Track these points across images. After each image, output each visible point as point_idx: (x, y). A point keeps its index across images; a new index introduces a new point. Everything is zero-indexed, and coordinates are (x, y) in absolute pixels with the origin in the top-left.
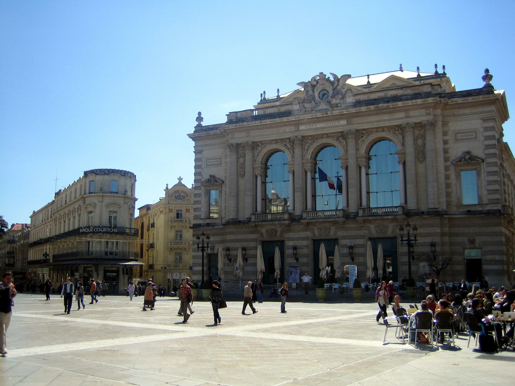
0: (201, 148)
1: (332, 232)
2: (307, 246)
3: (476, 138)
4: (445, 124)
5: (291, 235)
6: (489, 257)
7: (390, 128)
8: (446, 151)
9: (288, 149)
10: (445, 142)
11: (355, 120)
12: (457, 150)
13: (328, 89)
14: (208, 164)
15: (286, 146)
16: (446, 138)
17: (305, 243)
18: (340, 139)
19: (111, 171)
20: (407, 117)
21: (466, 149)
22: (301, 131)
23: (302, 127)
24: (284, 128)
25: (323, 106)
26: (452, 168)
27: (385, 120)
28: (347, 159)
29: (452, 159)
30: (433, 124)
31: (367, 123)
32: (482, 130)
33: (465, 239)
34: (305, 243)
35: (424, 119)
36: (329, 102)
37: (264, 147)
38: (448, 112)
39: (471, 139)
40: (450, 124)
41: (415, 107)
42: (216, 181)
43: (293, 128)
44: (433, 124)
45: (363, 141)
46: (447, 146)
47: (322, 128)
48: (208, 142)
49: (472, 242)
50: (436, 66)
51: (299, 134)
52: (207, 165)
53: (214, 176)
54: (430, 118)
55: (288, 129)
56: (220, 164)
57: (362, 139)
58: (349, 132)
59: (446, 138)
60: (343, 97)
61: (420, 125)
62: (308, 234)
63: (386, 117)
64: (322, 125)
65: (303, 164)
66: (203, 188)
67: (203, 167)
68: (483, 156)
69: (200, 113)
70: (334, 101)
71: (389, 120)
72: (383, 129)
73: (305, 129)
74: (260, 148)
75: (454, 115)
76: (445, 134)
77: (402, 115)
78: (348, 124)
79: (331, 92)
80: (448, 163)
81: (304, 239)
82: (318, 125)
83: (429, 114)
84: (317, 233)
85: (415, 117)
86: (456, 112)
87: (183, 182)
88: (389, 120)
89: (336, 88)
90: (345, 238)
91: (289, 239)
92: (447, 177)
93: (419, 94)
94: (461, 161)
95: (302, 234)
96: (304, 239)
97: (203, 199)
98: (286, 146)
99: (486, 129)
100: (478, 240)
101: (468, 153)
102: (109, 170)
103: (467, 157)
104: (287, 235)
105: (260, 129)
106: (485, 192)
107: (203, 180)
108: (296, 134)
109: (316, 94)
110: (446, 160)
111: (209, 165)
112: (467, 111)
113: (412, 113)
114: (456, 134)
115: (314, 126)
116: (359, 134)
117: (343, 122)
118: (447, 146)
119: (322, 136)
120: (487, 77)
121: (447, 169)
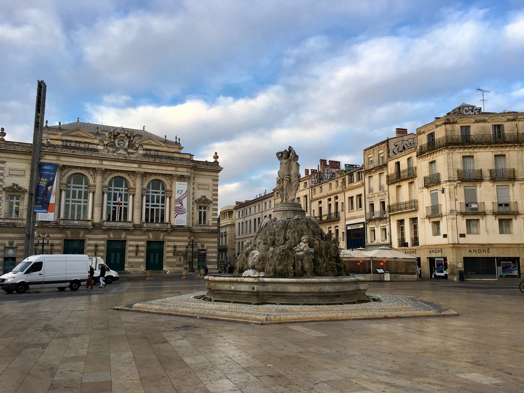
1: (123, 236)
2: (103, 245)
3: (208, 189)
4: (194, 178)
5: (91, 236)
6: (210, 255)
7: (163, 175)
9: (91, 175)
11: (144, 166)
14: (11, 173)
16: (194, 186)
25: (121, 151)
26: (195, 204)
28: (135, 189)
29: (196, 198)
32: (212, 185)
34: (103, 242)
36: (126, 150)
37: (70, 171)
38: (196, 172)
39: (206, 189)
41: (182, 166)
42: (20, 189)
43: (98, 162)
44: (189, 178)
48: (13, 156)
49: (203, 246)
50: (176, 137)
51: (103, 167)
52: (10, 174)
53: (17, 185)
54: (189, 174)
55: (94, 162)
56: (24, 175)
57: (145, 178)
59: (194, 186)
60: (137, 149)
62: (105, 236)
63: (164, 168)
66: (4, 193)
67: (5, 175)
70: (130, 150)
72: (160, 174)
77: (173, 169)
79: (127, 143)
82: (118, 164)
89: (132, 141)
90: (131, 240)
91: (90, 239)
92: (193, 209)
93: (184, 158)
95: (100, 236)
100: (206, 245)
104: (88, 236)
105: (70, 157)
106: (211, 219)
107: (4, 187)
108: (100, 166)
109: (116, 142)
111: (13, 175)
113: (179, 169)
115: (114, 164)
116: (145, 175)
117: (136, 165)
119: (118, 171)
120: (216, 157)
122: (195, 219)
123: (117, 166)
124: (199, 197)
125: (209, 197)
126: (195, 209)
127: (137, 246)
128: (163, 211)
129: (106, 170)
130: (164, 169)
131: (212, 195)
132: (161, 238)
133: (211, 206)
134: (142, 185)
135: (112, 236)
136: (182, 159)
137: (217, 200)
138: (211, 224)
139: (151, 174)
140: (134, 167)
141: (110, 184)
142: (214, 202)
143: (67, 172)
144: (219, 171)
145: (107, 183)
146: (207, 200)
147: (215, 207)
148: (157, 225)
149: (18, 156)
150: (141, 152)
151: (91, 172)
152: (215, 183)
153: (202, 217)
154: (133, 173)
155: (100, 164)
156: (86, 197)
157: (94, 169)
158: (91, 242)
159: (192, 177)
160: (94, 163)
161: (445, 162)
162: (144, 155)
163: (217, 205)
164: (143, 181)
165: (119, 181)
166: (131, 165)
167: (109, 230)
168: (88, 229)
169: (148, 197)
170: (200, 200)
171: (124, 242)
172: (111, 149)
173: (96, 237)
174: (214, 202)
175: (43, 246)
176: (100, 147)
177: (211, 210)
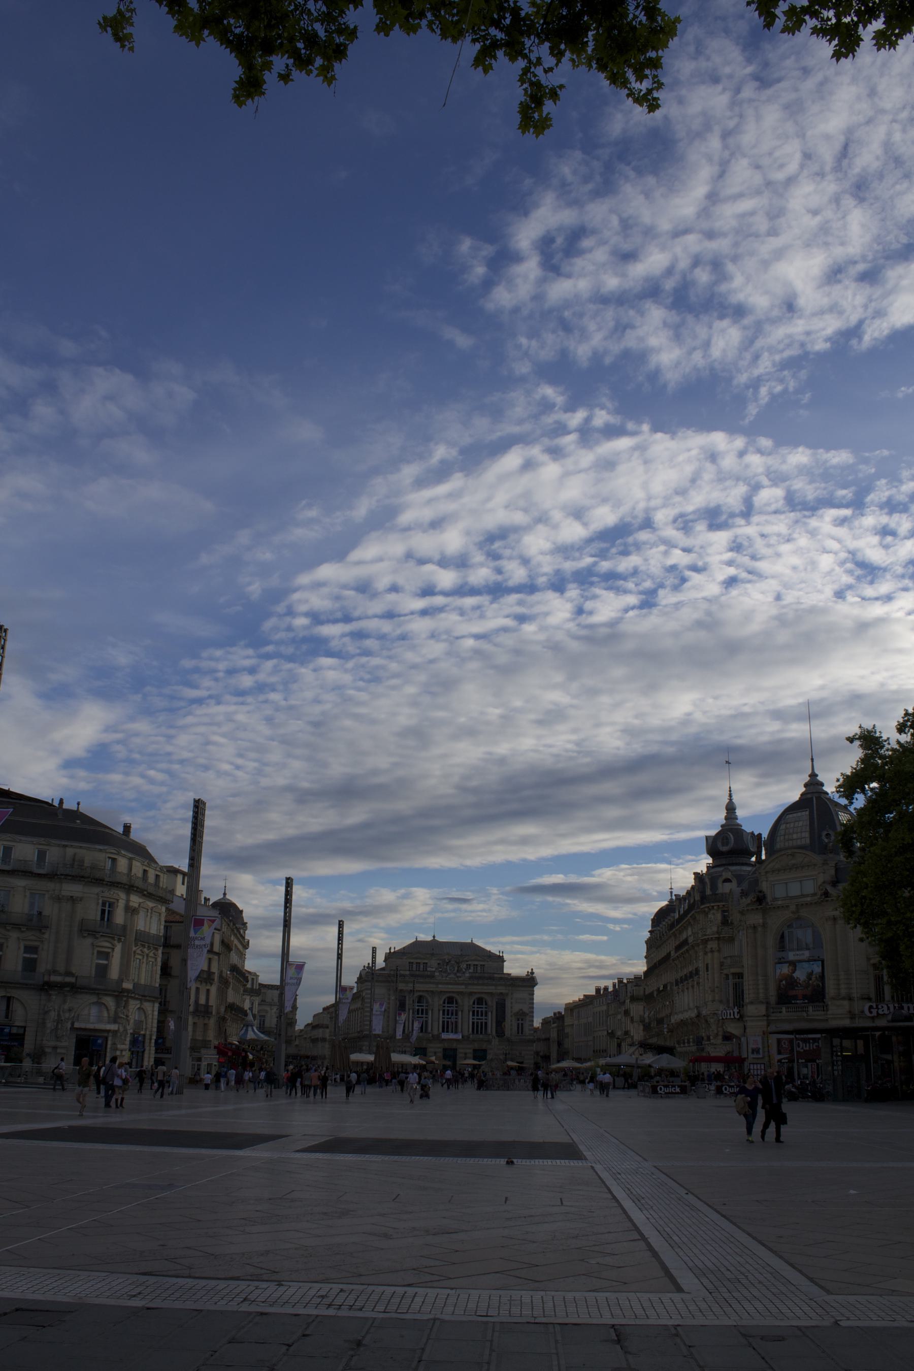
25: (452, 976)
30: (507, 994)
35: (503, 991)
36: (455, 974)
44: (507, 994)
72: (482, 993)
73: (441, 987)
116: (471, 994)
120: (532, 973)
125: (526, 1010)
127: (466, 1054)
128: (486, 1023)
132: (484, 1047)
136: (501, 978)
139: (475, 993)
140: (462, 988)
141: (444, 1003)
145: (442, 1002)
148: (481, 1036)
150: (467, 975)
153: (520, 1029)
154: (461, 993)
156: (427, 1014)
157: (432, 992)
160: (431, 987)
161: (637, 1009)
162: (470, 978)
165: (450, 1000)
169: (473, 1012)
171: (455, 1050)
172: (444, 975)
176: (437, 974)
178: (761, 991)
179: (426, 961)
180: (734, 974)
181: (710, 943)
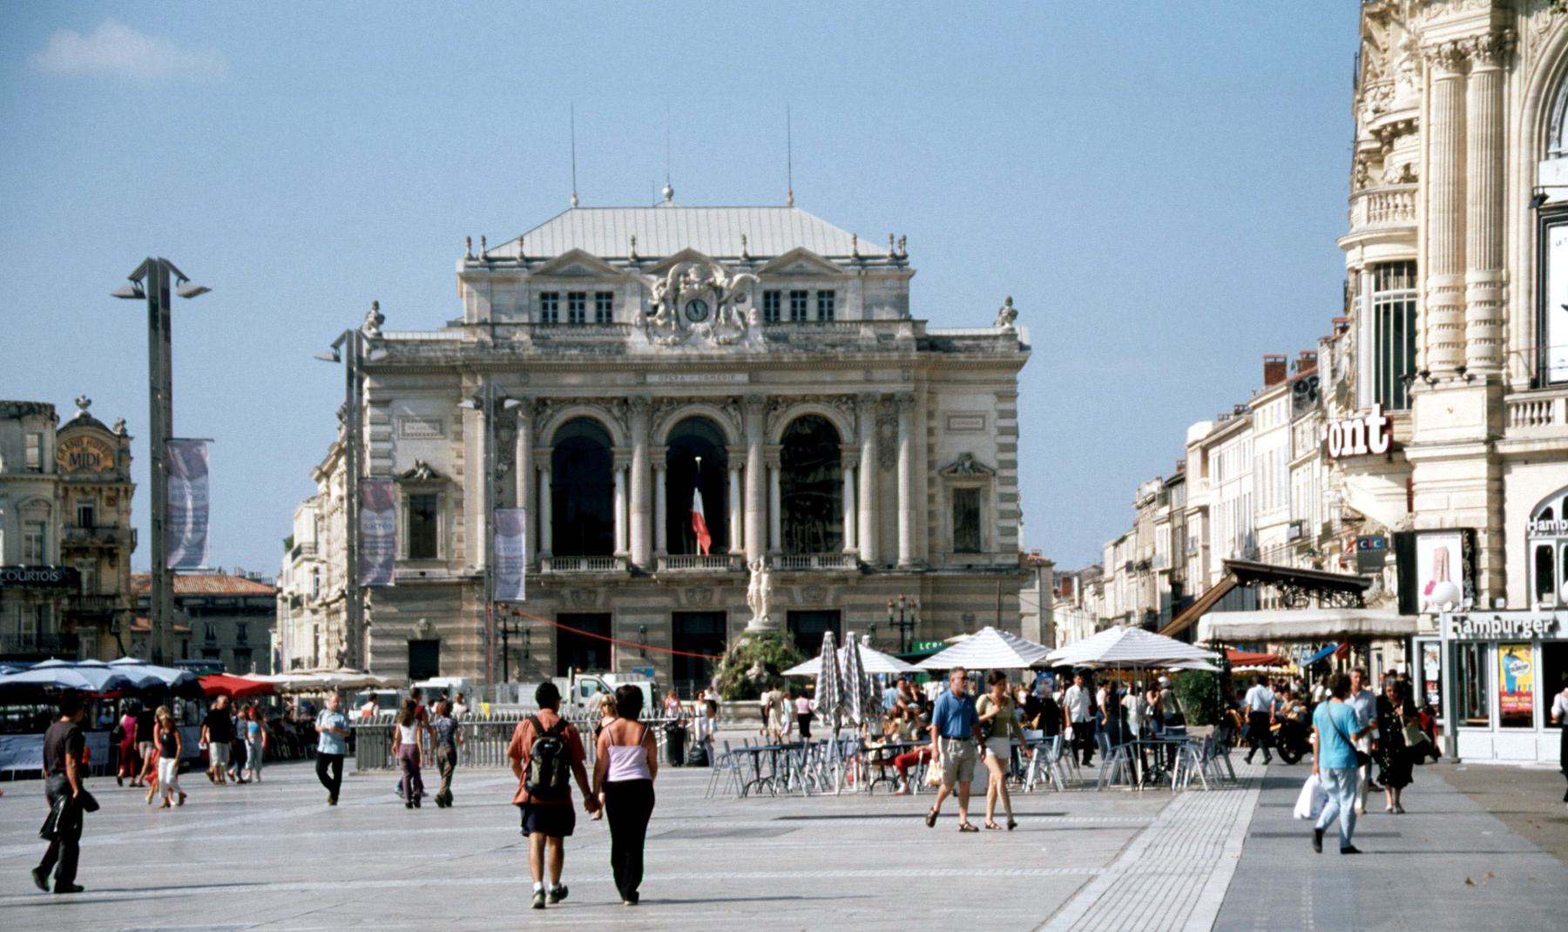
0: (386, 395)
5: (628, 601)
8: (930, 449)
9: (616, 419)
10: (930, 432)
11: (765, 375)
12: (951, 448)
13: (706, 300)
15: (609, 411)
16: (934, 424)
17: (660, 619)
18: (730, 409)
19: (25, 409)
20: (869, 381)
21: (965, 449)
22: (651, 385)
23: (652, 378)
24: (613, 375)
26: (939, 480)
27: (824, 383)
29: (940, 464)
31: (792, 383)
32: (995, 415)
33: (959, 615)
34: (660, 619)
35: (897, 388)
37: (558, 411)
40: (940, 397)
43: (631, 378)
44: (911, 400)
45: (778, 417)
46: (933, 440)
47: (694, 384)
48: (407, 380)
53: (425, 466)
54: (910, 387)
55: (620, 378)
58: (754, 399)
59: (934, 424)
61: (888, 398)
62: (667, 601)
63: (828, 376)
64: (695, 378)
65: (650, 454)
68: (994, 465)
69: (376, 305)
71: (832, 383)
72: (817, 399)
74: (549, 412)
75: (947, 381)
76: (931, 415)
77: (858, 375)
78: (752, 381)
80: (934, 473)
81: (655, 610)
82: (688, 378)
83: (906, 380)
84: (684, 601)
85: (882, 382)
86: (952, 375)
87: (95, 412)
88: (832, 383)
92: (931, 498)
94: (955, 471)
95: (654, 601)
96: (655, 610)
97: (399, 512)
98: (609, 411)
99: (1003, 414)
101: (969, 456)
102: (18, 405)
103: (967, 464)
107: (396, 471)
108: (639, 391)
110: (931, 465)
112: (970, 376)
114: (949, 418)
115: (679, 378)
117: (742, 377)
118: (933, 440)
121: (931, 482)
122: (939, 533)
123: (684, 385)
124: (954, 457)
125: (987, 454)
126: (939, 498)
129: (658, 402)
130: (828, 379)
131: (995, 448)
133: (996, 488)
134: (765, 434)
135: (684, 601)
137: (1013, 464)
138: (995, 548)
142: (1006, 473)
143: (552, 416)
144: (1018, 366)
146: (977, 468)
147: (1010, 490)
149: (420, 381)
151: (615, 411)
152: (1008, 406)
155: (639, 384)
158: (629, 619)
159: (925, 396)
163: (1013, 481)
164: (765, 420)
166: (728, 378)
167: (670, 583)
168: (616, 582)
170: (955, 469)
173: (640, 603)
174: (1006, 473)
175: (505, 639)
177: (993, 498)
178: (1474, 332)
179: (605, 288)
180: (1377, 267)
181: (1399, 143)
